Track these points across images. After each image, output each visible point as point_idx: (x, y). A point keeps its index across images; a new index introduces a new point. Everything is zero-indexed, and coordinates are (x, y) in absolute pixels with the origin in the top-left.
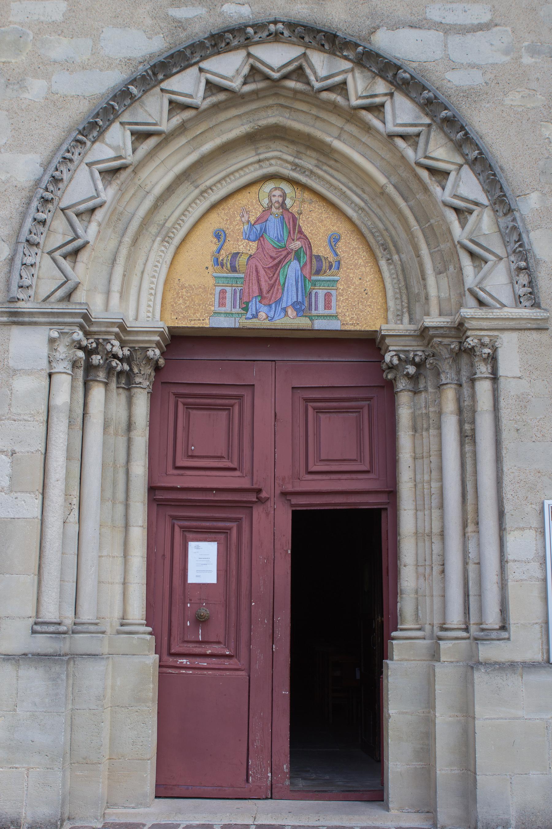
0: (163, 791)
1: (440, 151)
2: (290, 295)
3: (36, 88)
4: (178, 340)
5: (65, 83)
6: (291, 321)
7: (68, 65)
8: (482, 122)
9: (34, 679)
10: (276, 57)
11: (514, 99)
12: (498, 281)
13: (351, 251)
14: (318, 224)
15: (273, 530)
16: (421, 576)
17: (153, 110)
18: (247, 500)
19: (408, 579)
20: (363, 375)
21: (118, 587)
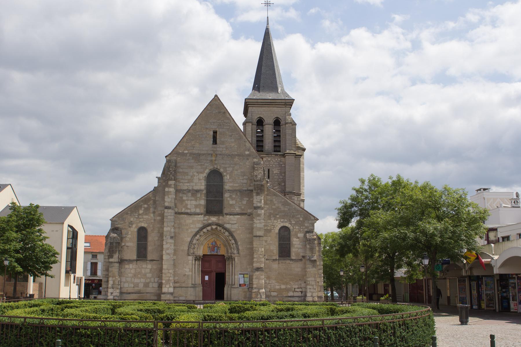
0: (203, 300)
1: (230, 238)
2: (216, 251)
3: (190, 230)
4: (204, 255)
5: (192, 230)
6: (215, 253)
7: (192, 228)
8: (235, 234)
9: (192, 289)
10: (214, 227)
11: (238, 232)
12: (235, 252)
13: (222, 246)
14: (218, 243)
15: (214, 275)
16: (228, 279)
17: (202, 233)
18: (211, 271)
19: (227, 280)
20: (223, 260)
21: (199, 281)
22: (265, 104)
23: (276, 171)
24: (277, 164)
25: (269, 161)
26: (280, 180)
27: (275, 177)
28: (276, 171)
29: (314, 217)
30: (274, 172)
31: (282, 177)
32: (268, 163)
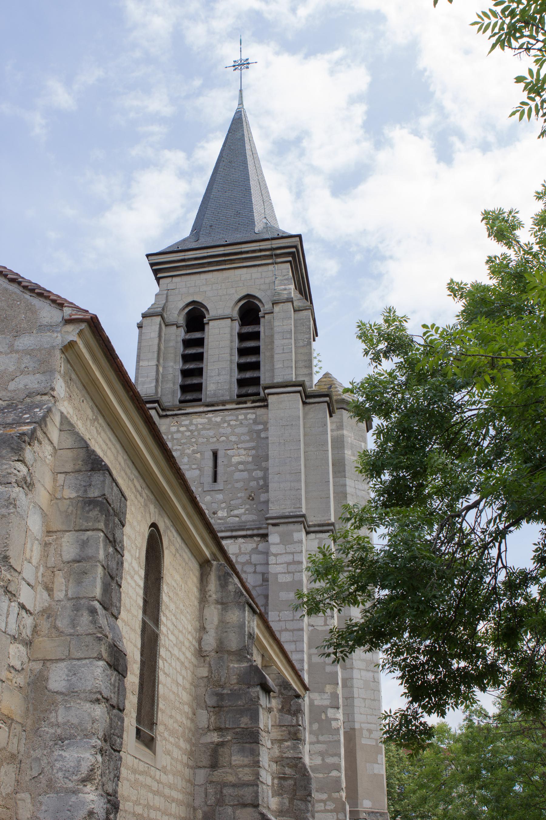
22: (210, 264)
23: (237, 456)
24: (244, 430)
25: (218, 424)
26: (253, 484)
27: (237, 475)
28: (237, 456)
29: (59, 303)
30: (235, 460)
31: (260, 474)
32: (211, 433)
